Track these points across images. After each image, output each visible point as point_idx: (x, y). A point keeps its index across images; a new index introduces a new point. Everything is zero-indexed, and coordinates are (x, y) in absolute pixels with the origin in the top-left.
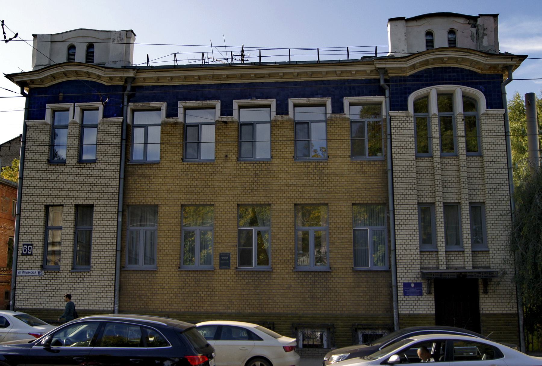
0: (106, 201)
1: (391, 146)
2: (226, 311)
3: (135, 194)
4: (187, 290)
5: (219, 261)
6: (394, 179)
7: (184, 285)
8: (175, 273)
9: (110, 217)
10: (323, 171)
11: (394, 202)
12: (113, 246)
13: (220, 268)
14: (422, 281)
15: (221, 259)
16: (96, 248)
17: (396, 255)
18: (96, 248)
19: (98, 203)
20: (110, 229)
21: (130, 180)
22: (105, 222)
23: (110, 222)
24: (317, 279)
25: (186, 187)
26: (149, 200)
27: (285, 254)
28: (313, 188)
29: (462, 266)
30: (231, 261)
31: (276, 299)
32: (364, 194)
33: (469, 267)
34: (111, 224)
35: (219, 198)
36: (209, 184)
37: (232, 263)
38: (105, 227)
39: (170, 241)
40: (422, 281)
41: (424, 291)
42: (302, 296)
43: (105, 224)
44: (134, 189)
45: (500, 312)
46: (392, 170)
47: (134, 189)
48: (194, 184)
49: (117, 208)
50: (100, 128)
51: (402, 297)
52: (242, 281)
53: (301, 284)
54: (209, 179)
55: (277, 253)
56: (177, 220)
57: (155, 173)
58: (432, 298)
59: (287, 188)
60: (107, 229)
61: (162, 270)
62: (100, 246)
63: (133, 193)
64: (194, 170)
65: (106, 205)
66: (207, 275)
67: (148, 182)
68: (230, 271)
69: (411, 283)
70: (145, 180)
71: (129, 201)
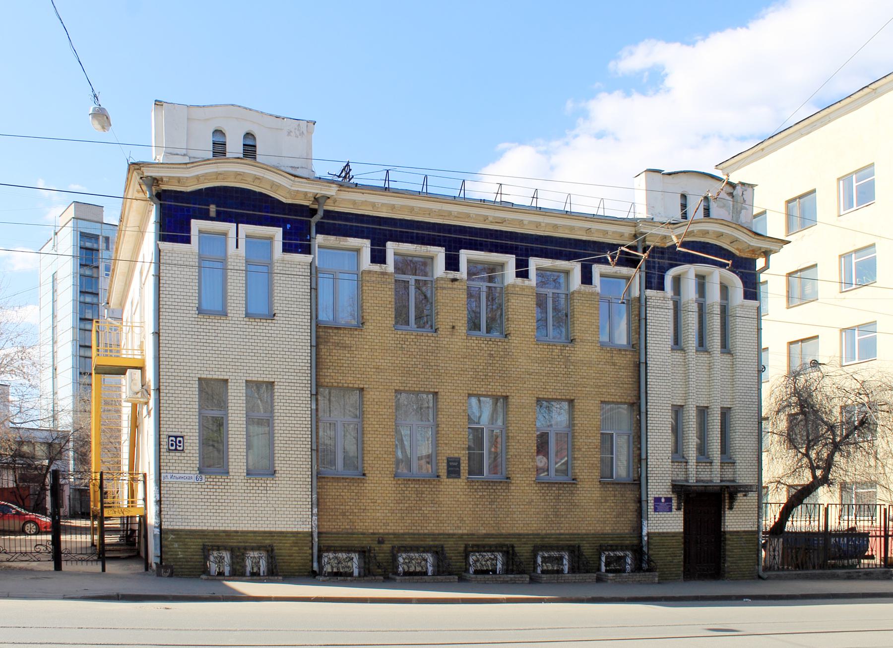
0: (293, 377)
1: (646, 334)
2: (456, 531)
3: (331, 371)
4: (406, 505)
5: (446, 468)
6: (649, 374)
7: (402, 498)
8: (390, 482)
9: (301, 402)
10: (570, 358)
11: (647, 403)
12: (306, 443)
13: (448, 477)
14: (673, 496)
15: (449, 466)
16: (282, 445)
17: (647, 464)
18: (282, 445)
19: (282, 380)
20: (302, 419)
21: (323, 350)
22: (293, 408)
23: (301, 409)
24: (561, 492)
25: (400, 365)
26: (350, 380)
27: (525, 460)
28: (559, 378)
29: (709, 479)
30: (462, 468)
31: (515, 516)
32: (613, 391)
33: (717, 480)
34: (302, 412)
35: (445, 384)
36: (431, 364)
37: (462, 471)
38: (293, 415)
39: (381, 439)
40: (673, 496)
41: (673, 507)
42: (544, 513)
43: (293, 412)
44: (329, 364)
45: (743, 529)
46: (646, 363)
47: (329, 364)
48: (411, 363)
49: (309, 389)
50: (279, 268)
51: (653, 513)
52: (475, 493)
53: (543, 498)
54: (431, 358)
55: (516, 460)
56: (391, 411)
57: (357, 343)
58: (681, 514)
59: (528, 376)
60: (296, 419)
61: (372, 478)
62: (288, 442)
63: (327, 369)
64: (412, 343)
65: (293, 384)
66: (431, 486)
67: (349, 355)
68: (460, 480)
69: (661, 498)
70: (344, 352)
71: (323, 380)
